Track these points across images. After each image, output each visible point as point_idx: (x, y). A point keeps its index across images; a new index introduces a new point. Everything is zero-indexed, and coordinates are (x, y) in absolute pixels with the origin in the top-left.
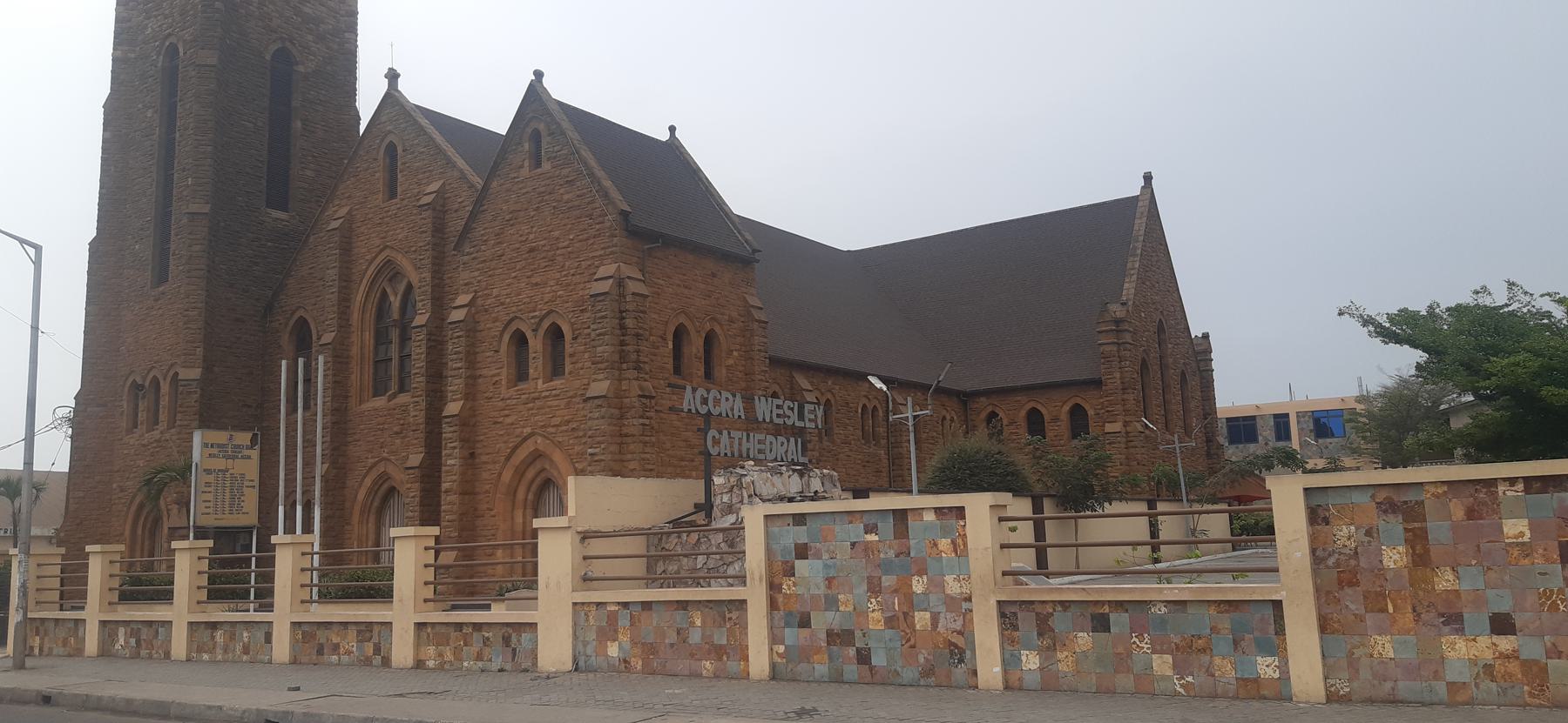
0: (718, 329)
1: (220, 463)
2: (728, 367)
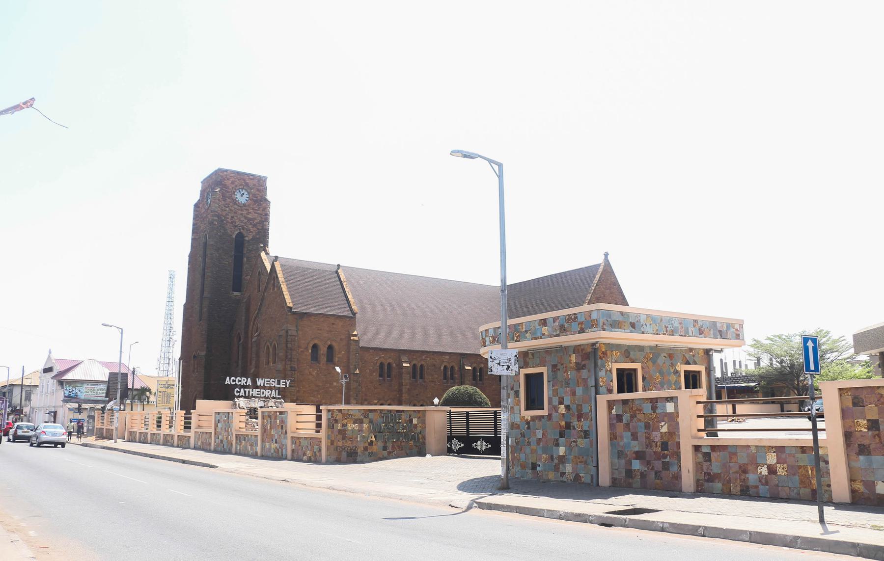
0: (335, 344)
1: (164, 390)
2: (339, 358)
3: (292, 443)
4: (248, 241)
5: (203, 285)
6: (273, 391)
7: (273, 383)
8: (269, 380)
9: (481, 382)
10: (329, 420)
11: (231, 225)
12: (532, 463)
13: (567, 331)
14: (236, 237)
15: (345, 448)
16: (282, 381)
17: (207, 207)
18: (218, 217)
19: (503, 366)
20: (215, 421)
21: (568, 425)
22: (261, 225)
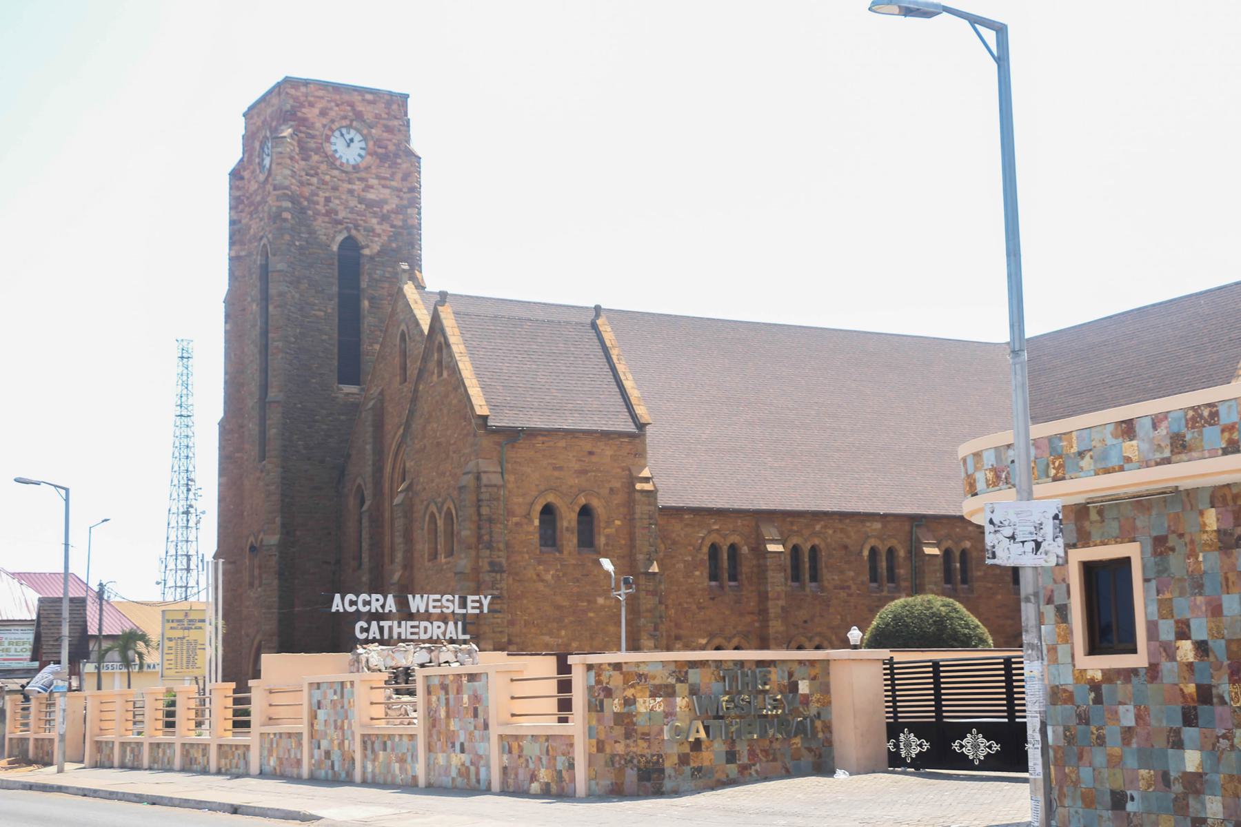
0: (595, 503)
1: (179, 633)
2: (608, 536)
3: (502, 750)
4: (371, 258)
5: (265, 371)
6: (451, 624)
7: (450, 604)
8: (438, 597)
9: (966, 586)
10: (590, 689)
11: (327, 219)
12: (1113, 793)
13: (1190, 450)
14: (339, 248)
15: (632, 758)
16: (470, 598)
17: (262, 178)
18: (293, 203)
19: (1023, 542)
20: (310, 704)
21: (1205, 694)
22: (401, 217)
